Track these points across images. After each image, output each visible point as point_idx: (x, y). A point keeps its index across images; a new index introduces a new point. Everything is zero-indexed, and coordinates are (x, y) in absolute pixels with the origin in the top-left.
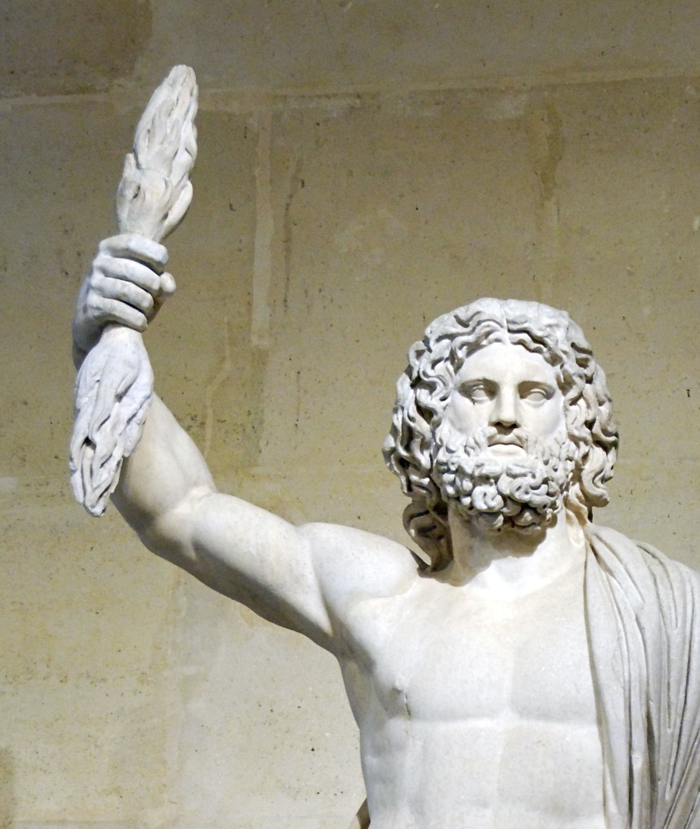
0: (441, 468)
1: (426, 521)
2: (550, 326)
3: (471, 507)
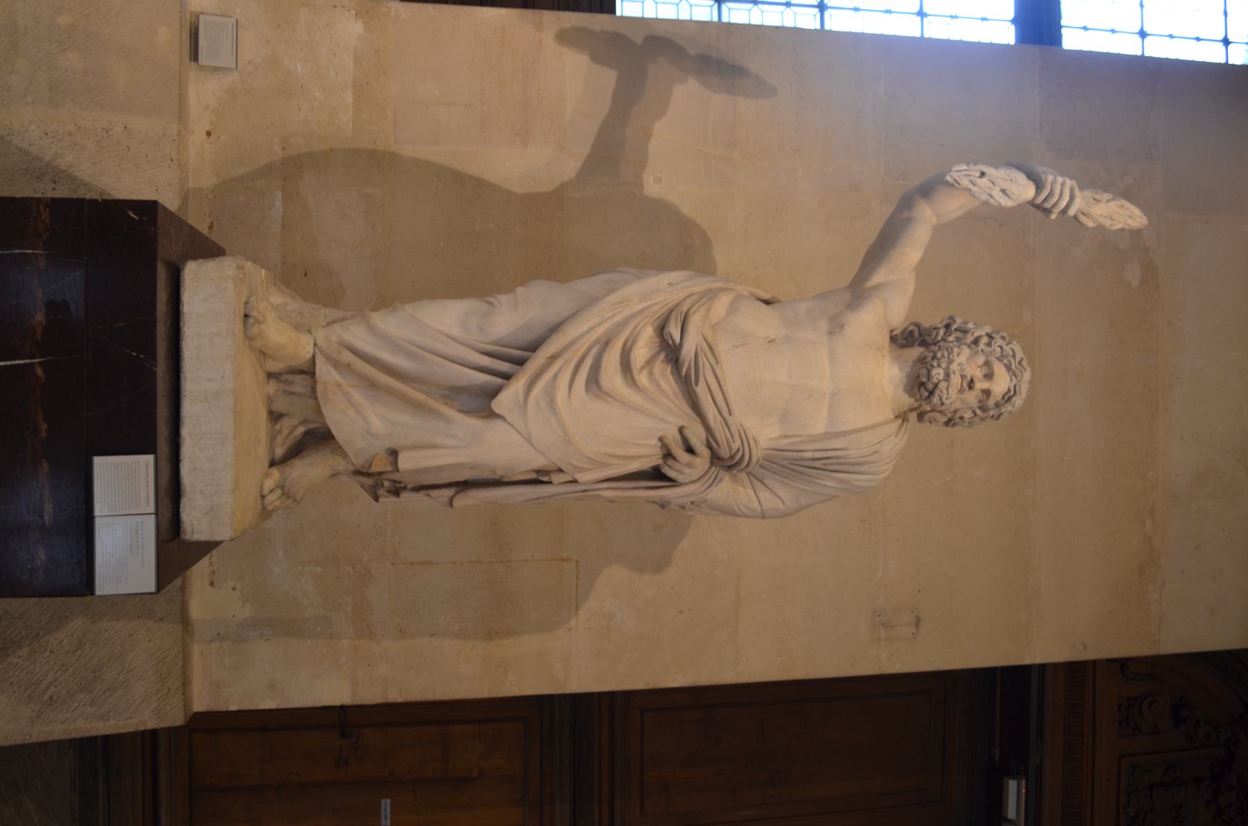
1: (916, 334)
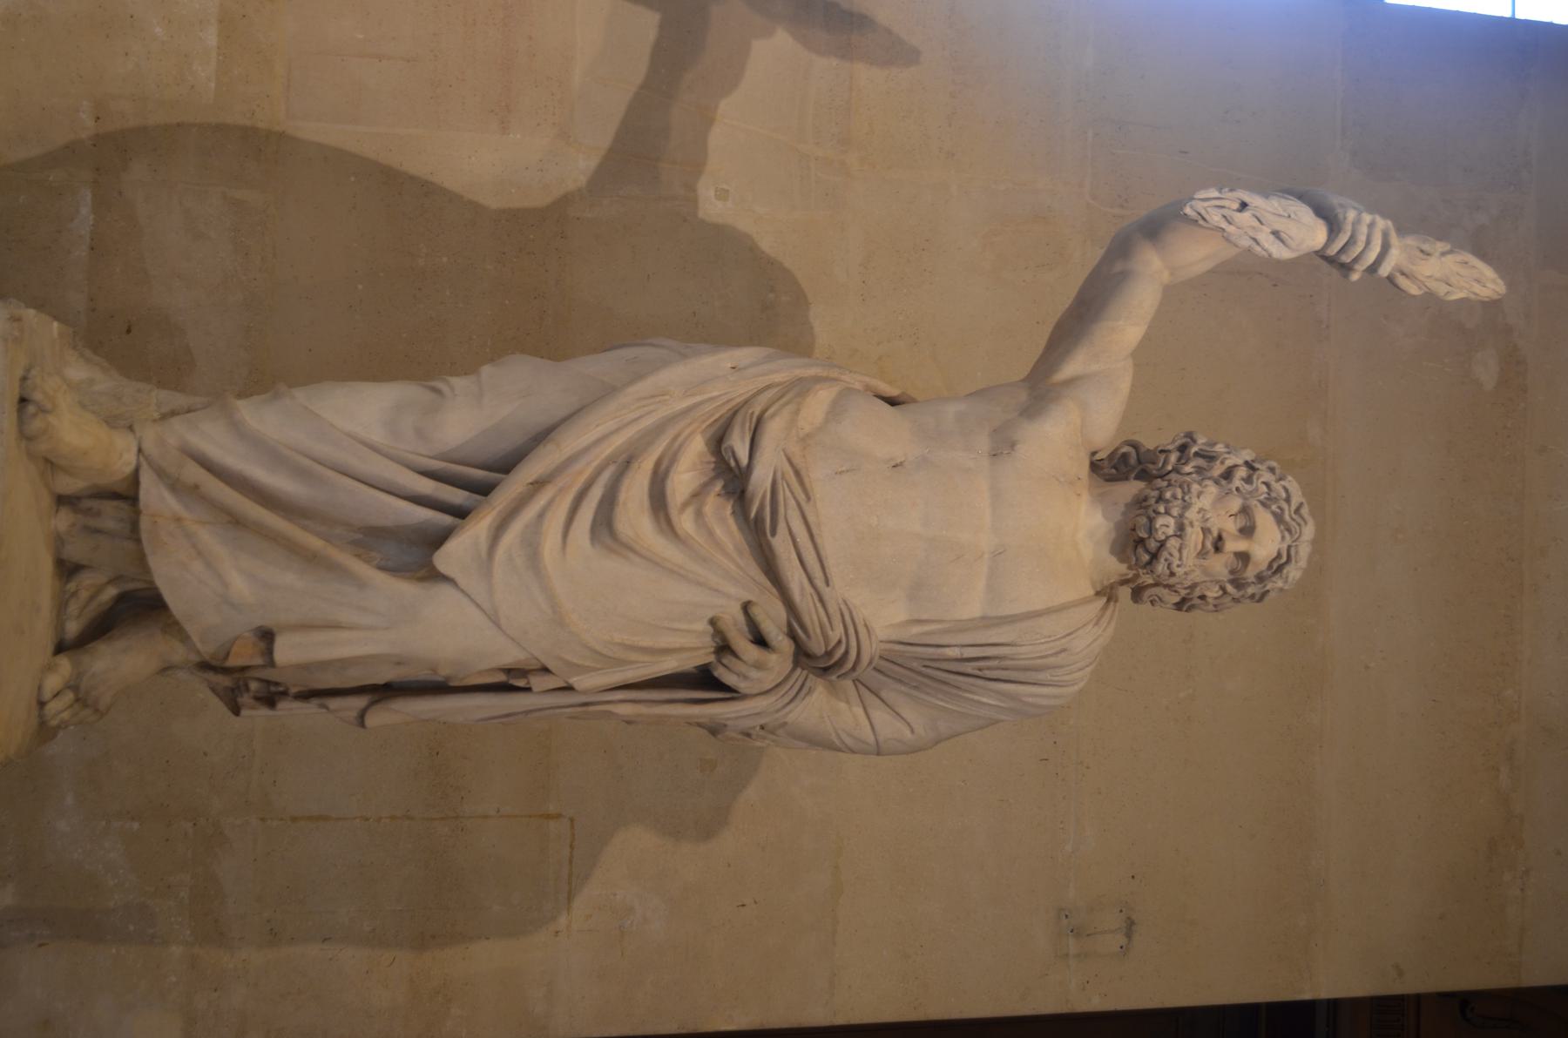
0: (1186, 489)
1: (1133, 460)
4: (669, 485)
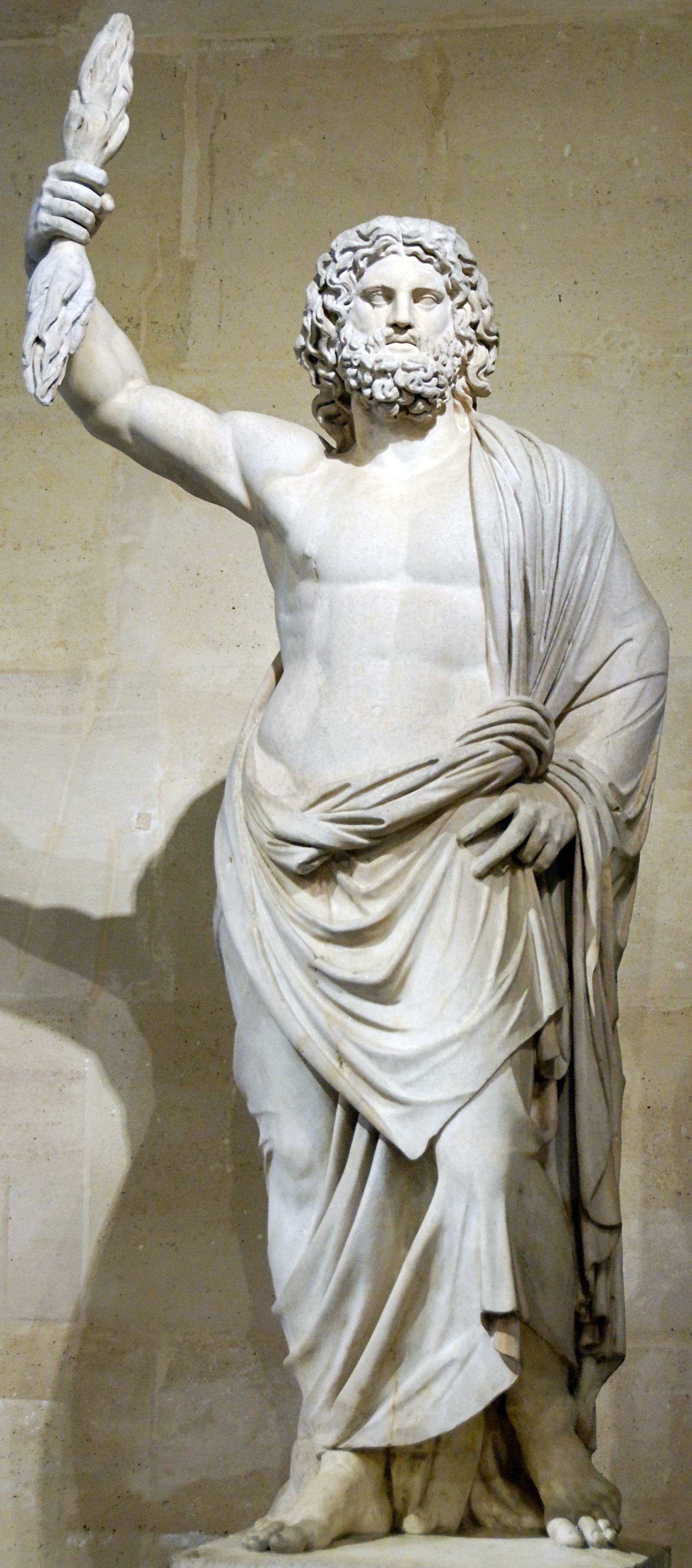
0: (346, 363)
1: (331, 409)
2: (440, 240)
3: (371, 397)
4: (338, 927)
